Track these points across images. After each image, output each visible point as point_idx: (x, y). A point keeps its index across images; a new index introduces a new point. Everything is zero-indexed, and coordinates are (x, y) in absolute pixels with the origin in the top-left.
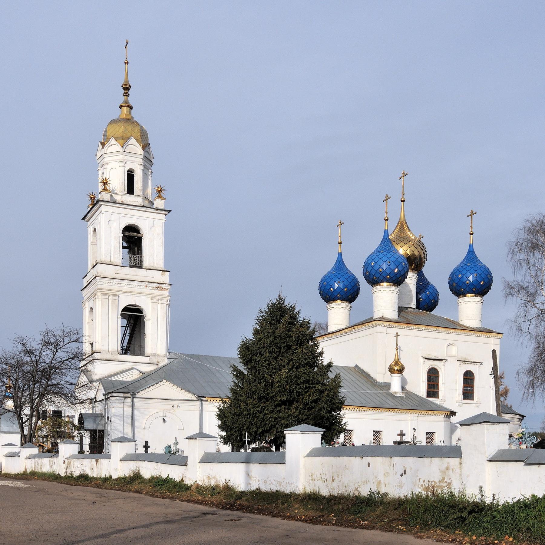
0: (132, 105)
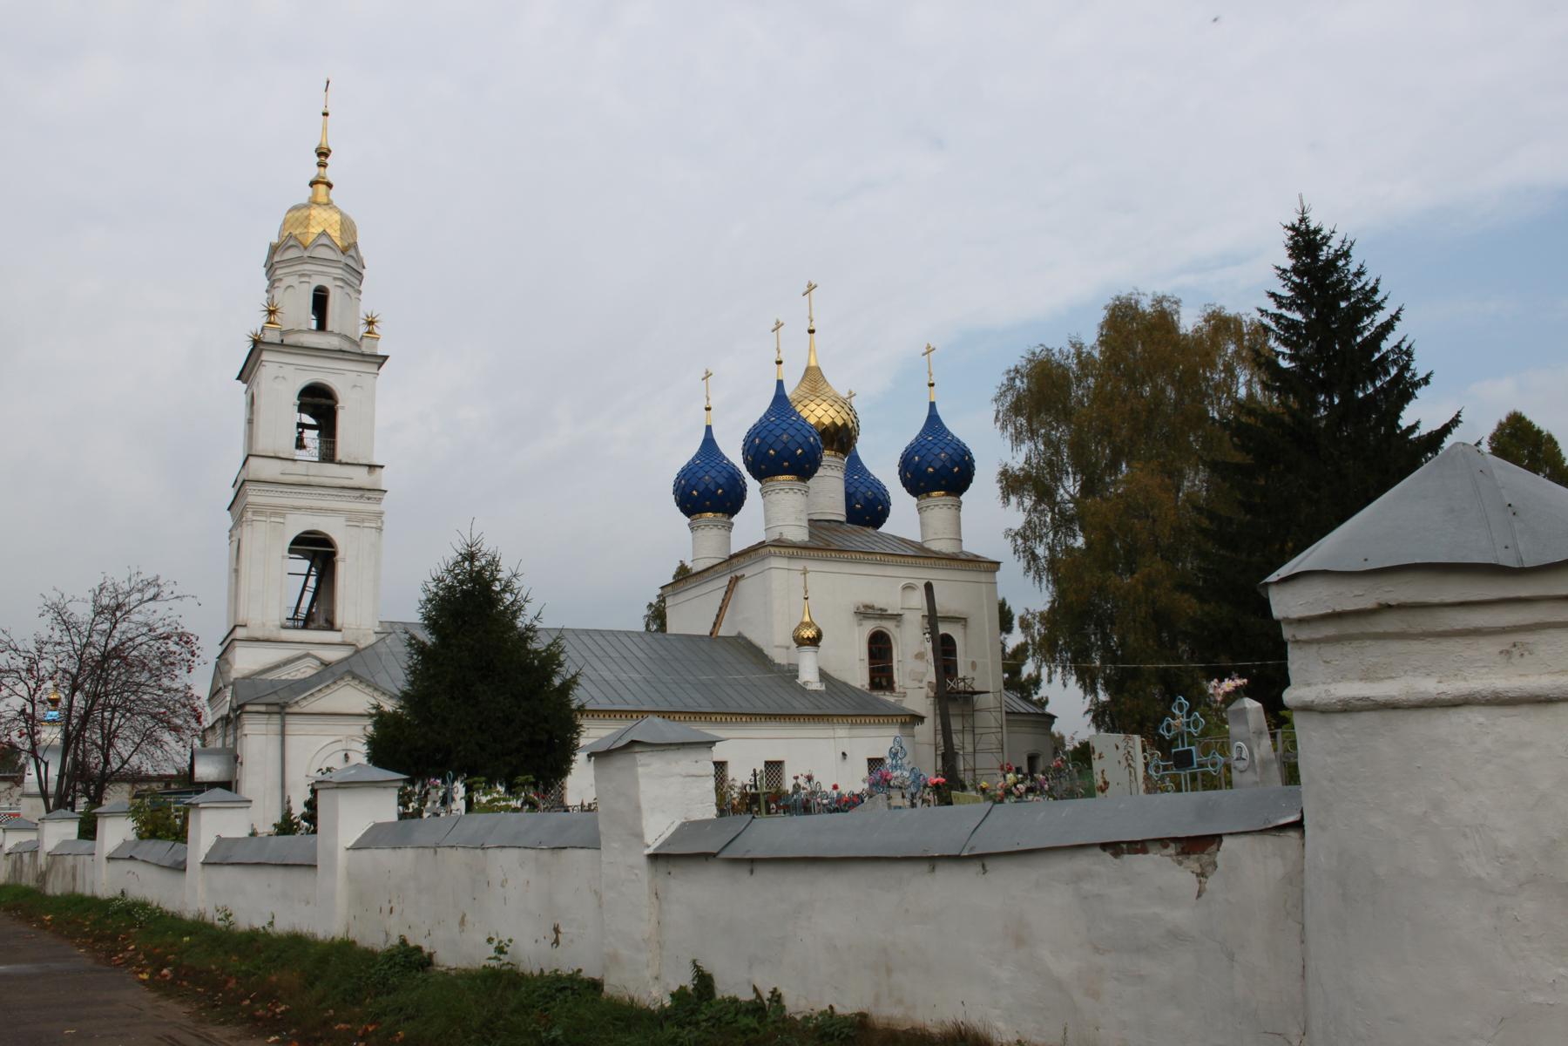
0: (332, 181)
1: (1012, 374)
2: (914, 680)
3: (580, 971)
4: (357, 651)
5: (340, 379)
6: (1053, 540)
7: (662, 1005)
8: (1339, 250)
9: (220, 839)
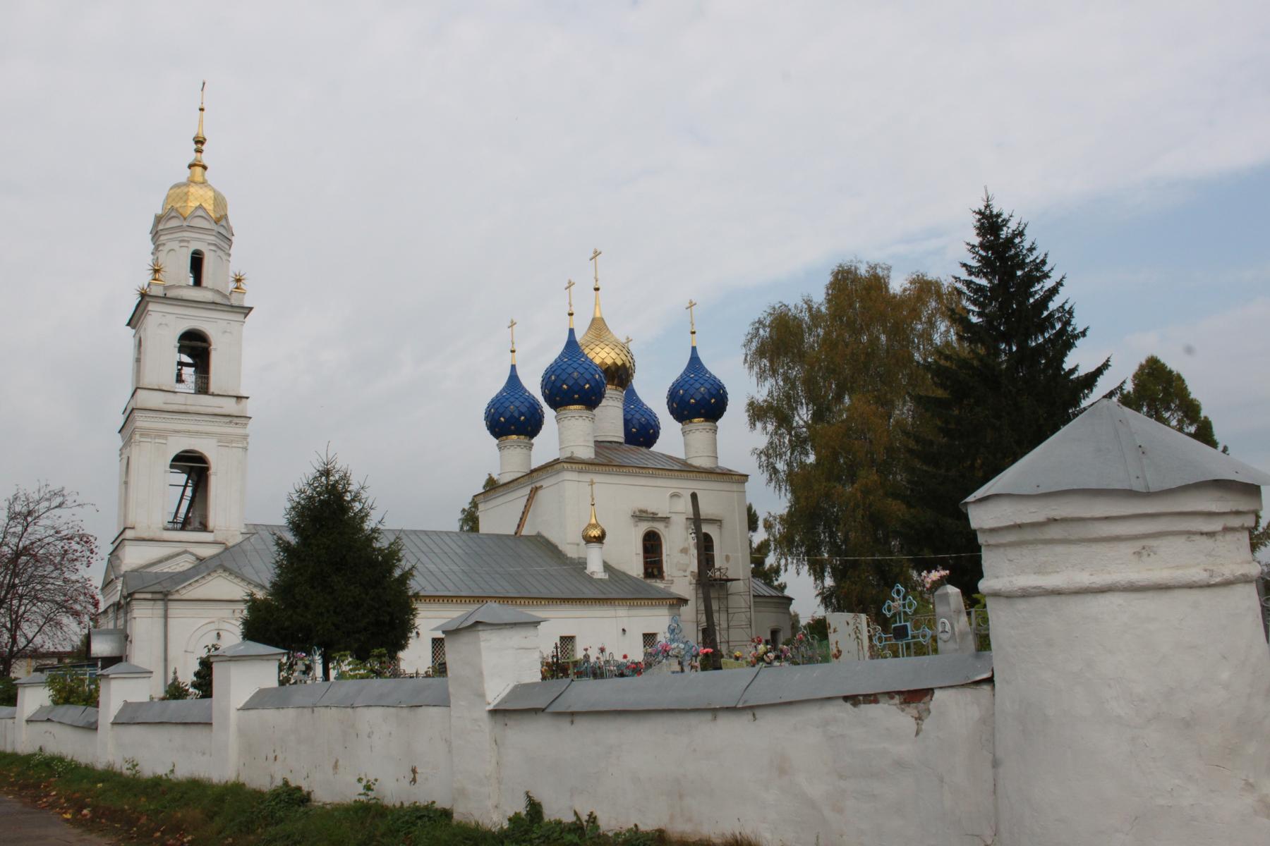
1: (757, 325)
2: (679, 570)
3: (434, 802)
4: (227, 549)
5: (213, 326)
6: (790, 458)
7: (502, 827)
8: (1016, 230)
9: (126, 704)
